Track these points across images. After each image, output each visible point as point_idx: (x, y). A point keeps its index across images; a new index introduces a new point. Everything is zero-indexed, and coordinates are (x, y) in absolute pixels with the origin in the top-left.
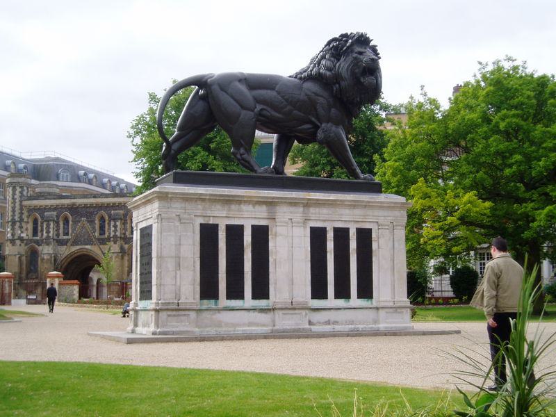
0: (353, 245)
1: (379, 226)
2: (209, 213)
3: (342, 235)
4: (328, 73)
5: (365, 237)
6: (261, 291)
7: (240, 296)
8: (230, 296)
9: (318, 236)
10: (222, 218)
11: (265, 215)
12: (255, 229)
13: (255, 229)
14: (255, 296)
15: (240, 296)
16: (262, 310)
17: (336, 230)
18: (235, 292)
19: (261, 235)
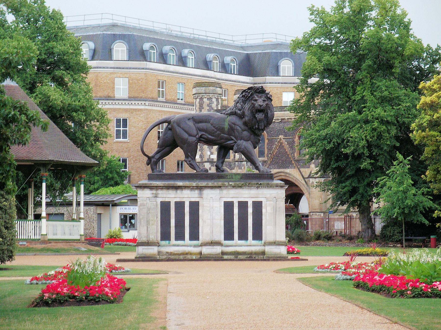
0: (250, 210)
1: (267, 199)
2: (165, 196)
3: (243, 205)
4: (239, 112)
5: (258, 206)
6: (195, 236)
7: (183, 238)
8: (177, 239)
9: (228, 206)
10: (172, 197)
11: (197, 195)
12: (191, 203)
13: (191, 203)
14: (191, 239)
15: (183, 238)
16: (195, 246)
17: (239, 203)
18: (180, 236)
19: (195, 206)
